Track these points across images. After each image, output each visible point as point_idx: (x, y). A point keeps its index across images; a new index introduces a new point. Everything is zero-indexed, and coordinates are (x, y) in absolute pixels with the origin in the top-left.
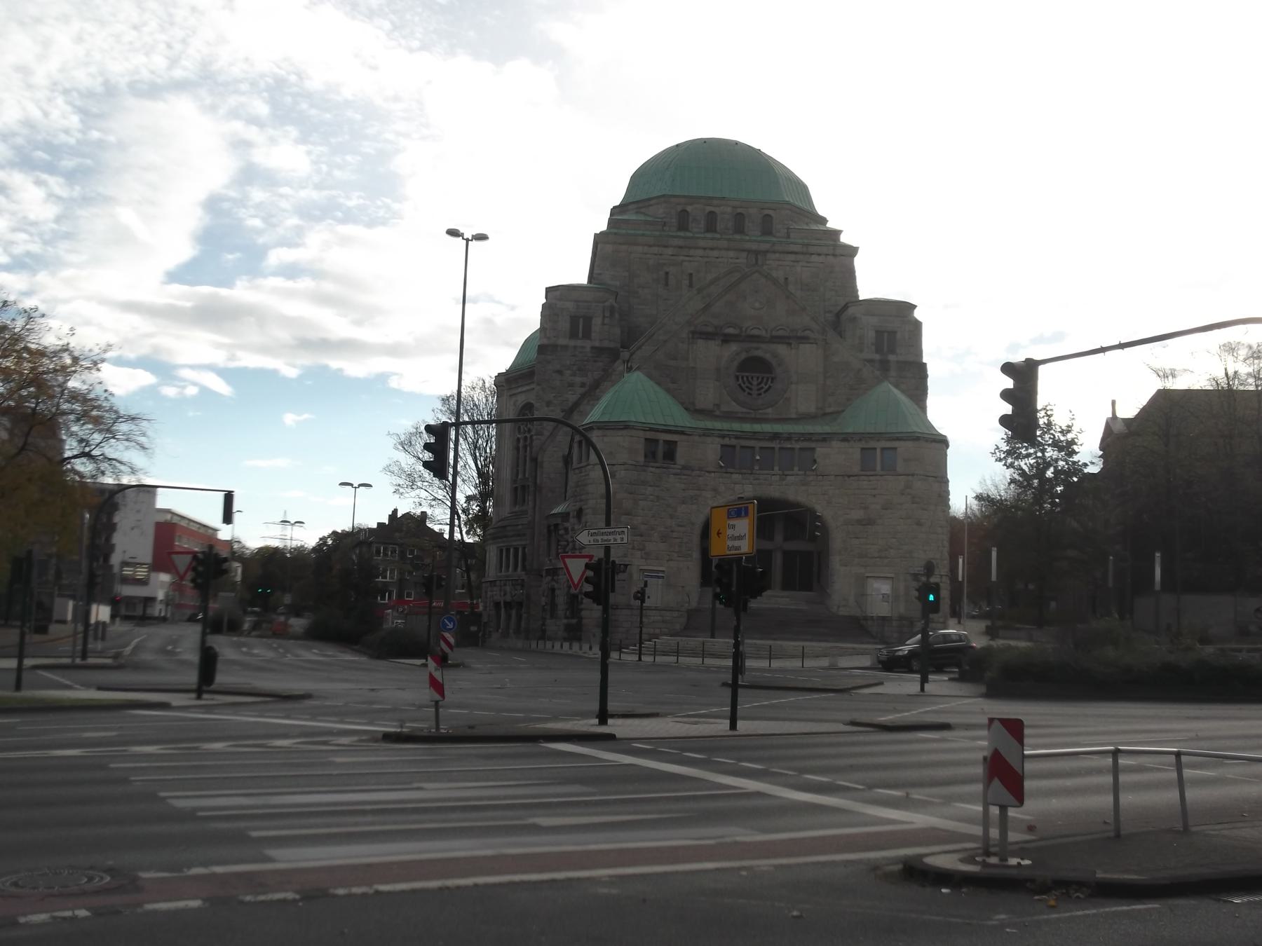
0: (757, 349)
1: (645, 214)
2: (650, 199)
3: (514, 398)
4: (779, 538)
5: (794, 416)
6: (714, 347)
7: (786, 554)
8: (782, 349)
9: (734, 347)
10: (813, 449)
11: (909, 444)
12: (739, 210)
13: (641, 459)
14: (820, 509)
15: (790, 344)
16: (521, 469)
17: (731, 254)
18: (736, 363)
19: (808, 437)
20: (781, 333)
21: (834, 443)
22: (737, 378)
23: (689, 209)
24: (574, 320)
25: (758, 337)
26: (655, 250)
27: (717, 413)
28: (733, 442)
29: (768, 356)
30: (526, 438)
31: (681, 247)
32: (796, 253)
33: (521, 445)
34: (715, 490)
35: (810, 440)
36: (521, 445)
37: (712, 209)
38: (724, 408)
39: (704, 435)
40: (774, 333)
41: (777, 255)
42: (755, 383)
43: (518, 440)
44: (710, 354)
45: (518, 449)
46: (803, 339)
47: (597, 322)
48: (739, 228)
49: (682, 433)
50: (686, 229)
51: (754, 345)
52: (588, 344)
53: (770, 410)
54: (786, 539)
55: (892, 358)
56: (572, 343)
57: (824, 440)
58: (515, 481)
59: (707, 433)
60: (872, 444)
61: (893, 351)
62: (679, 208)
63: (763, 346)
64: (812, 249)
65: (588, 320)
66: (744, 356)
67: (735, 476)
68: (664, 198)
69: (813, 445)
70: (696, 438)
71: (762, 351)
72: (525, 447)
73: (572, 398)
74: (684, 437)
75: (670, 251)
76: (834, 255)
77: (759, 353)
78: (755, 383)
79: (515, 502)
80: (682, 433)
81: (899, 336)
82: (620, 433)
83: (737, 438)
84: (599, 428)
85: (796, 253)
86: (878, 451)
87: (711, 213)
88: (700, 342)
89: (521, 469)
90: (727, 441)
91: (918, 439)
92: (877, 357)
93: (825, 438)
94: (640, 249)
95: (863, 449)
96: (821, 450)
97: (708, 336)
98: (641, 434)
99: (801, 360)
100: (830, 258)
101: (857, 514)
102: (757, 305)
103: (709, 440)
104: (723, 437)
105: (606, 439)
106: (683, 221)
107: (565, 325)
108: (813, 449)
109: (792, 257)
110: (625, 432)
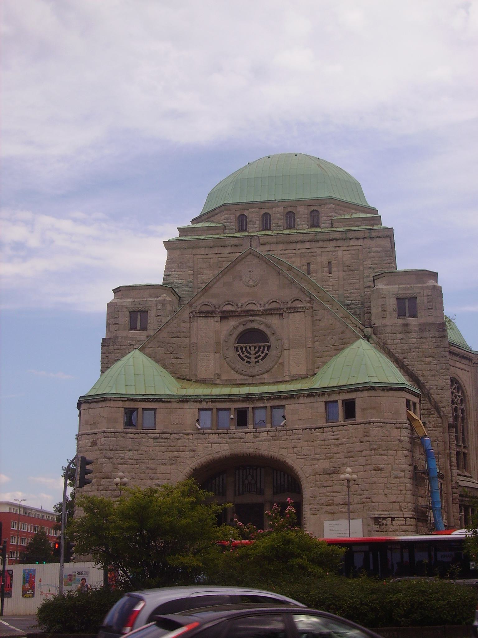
0: (252, 321)
1: (212, 222)
2: (215, 209)
4: (268, 492)
5: (287, 379)
6: (213, 323)
8: (274, 321)
9: (232, 323)
10: (283, 406)
11: (366, 394)
12: (289, 210)
13: (120, 427)
14: (290, 461)
15: (281, 314)
17: (281, 247)
18: (234, 336)
19: (278, 396)
20: (274, 305)
21: (302, 400)
22: (237, 348)
23: (246, 213)
25: (253, 311)
26: (216, 250)
27: (218, 382)
28: (210, 405)
29: (262, 327)
31: (237, 246)
32: (337, 240)
34: (194, 451)
35: (279, 398)
37: (266, 211)
38: (224, 377)
39: (182, 401)
40: (267, 307)
41: (321, 243)
42: (253, 352)
44: (210, 330)
46: (293, 310)
47: (152, 313)
48: (291, 225)
49: (161, 401)
50: (245, 230)
51: (251, 318)
53: (266, 376)
55: (412, 321)
56: (132, 333)
57: (292, 397)
59: (184, 400)
61: (413, 315)
62: (238, 214)
63: (257, 318)
64: (350, 235)
65: (144, 312)
66: (241, 329)
67: (212, 436)
68: (225, 207)
69: (283, 403)
70: (175, 405)
71: (257, 324)
74: (162, 405)
75: (228, 250)
76: (372, 238)
77: (254, 325)
78: (253, 352)
80: (161, 401)
81: (418, 301)
82: (100, 404)
84: (85, 403)
85: (337, 240)
86: (340, 403)
87: (265, 214)
88: (201, 321)
90: (204, 405)
91: (373, 388)
92: (400, 321)
93: (293, 396)
94: (203, 251)
95: (326, 403)
96: (290, 406)
97: (207, 314)
98: (121, 404)
99: (290, 330)
100: (368, 242)
101: (325, 464)
102: (251, 283)
103: (186, 405)
104: (200, 401)
106: (242, 223)
107: (125, 319)
108: (283, 406)
109: (334, 243)
110: (103, 404)
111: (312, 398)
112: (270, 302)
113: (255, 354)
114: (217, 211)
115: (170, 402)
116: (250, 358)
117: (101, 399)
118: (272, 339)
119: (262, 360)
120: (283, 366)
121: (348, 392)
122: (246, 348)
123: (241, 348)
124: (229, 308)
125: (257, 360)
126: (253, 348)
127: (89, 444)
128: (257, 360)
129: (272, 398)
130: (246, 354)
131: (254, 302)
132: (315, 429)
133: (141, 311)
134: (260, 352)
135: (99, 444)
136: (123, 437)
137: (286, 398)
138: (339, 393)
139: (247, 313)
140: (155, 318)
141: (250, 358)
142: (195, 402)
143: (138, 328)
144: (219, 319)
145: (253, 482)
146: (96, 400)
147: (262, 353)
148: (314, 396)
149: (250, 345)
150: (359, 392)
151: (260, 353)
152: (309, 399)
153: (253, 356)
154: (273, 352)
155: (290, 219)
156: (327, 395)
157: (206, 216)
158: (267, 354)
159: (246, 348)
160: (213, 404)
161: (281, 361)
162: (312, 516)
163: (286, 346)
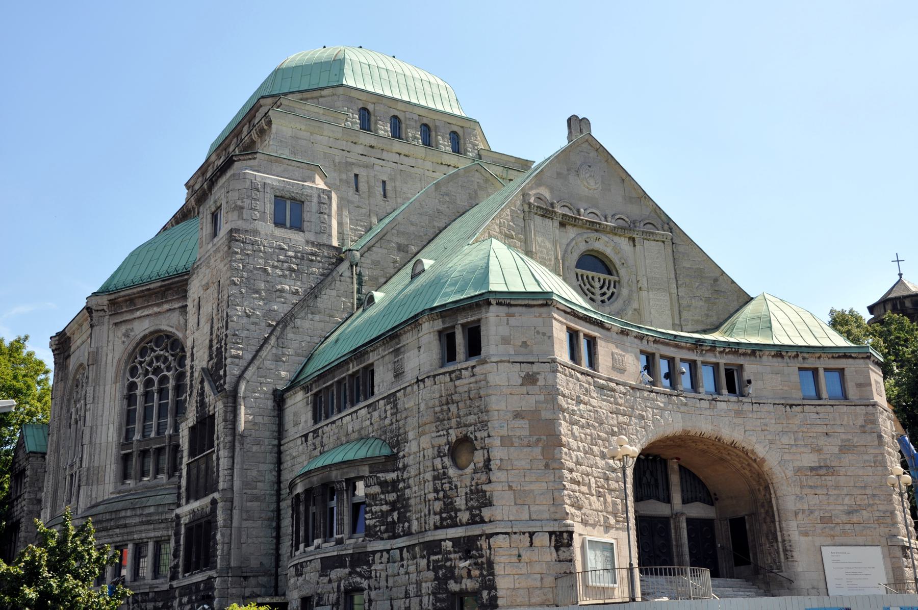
2: (322, 89)
3: (123, 328)
7: (690, 521)
9: (571, 232)
14: (761, 451)
16: (138, 426)
18: (575, 257)
22: (577, 275)
23: (370, 107)
24: (280, 200)
28: (651, 348)
29: (608, 251)
30: (149, 383)
31: (372, 147)
33: (140, 390)
35: (736, 353)
36: (140, 390)
43: (132, 386)
45: (130, 399)
52: (298, 238)
54: (685, 501)
56: (279, 232)
57: (753, 353)
58: (122, 446)
60: (811, 363)
66: (583, 247)
71: (604, 245)
72: (147, 396)
73: (280, 308)
78: (597, 285)
79: (125, 475)
83: (655, 342)
89: (138, 426)
95: (800, 369)
101: (809, 460)
105: (513, 321)
111: (780, 359)
112: (617, 217)
113: (601, 288)
114: (325, 92)
115: (608, 330)
116: (593, 294)
117: (540, 302)
118: (622, 271)
119: (609, 299)
120: (639, 314)
121: (833, 357)
122: (587, 277)
123: (582, 276)
124: (566, 211)
125: (602, 298)
126: (597, 280)
127: (520, 381)
128: (602, 298)
129: (727, 350)
130: (588, 286)
131: (597, 212)
132: (791, 406)
133: (293, 199)
134: (605, 288)
135: (541, 383)
136: (571, 376)
137: (745, 354)
138: (819, 358)
139: (594, 227)
140: (318, 215)
141: (593, 294)
142: (636, 337)
143: (288, 224)
144: (556, 224)
145: (653, 482)
146: (526, 302)
147: (608, 289)
148: (782, 357)
149: (594, 274)
150: (850, 361)
151: (605, 289)
152: (775, 359)
153: (598, 292)
154: (625, 292)
155: (427, 132)
156: (800, 358)
157: (299, 96)
158: (613, 294)
159: (587, 277)
160: (655, 346)
161: (635, 305)
162: (803, 539)
163: (643, 283)
